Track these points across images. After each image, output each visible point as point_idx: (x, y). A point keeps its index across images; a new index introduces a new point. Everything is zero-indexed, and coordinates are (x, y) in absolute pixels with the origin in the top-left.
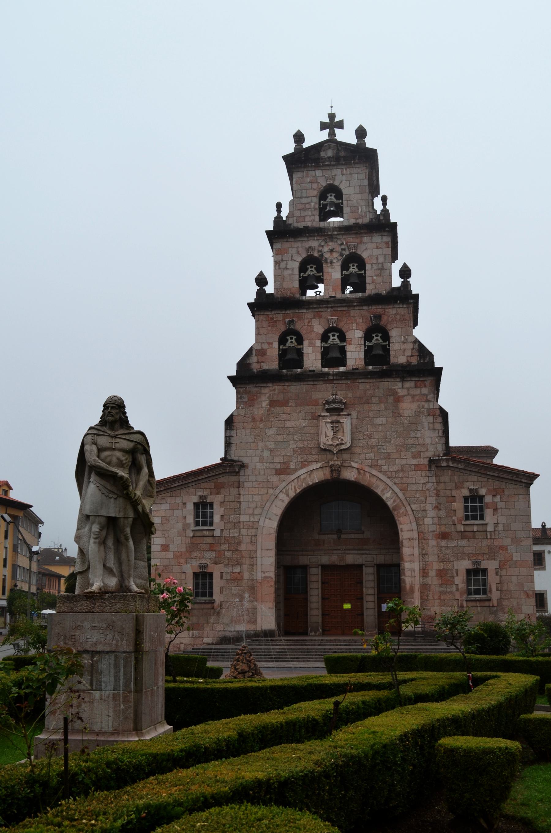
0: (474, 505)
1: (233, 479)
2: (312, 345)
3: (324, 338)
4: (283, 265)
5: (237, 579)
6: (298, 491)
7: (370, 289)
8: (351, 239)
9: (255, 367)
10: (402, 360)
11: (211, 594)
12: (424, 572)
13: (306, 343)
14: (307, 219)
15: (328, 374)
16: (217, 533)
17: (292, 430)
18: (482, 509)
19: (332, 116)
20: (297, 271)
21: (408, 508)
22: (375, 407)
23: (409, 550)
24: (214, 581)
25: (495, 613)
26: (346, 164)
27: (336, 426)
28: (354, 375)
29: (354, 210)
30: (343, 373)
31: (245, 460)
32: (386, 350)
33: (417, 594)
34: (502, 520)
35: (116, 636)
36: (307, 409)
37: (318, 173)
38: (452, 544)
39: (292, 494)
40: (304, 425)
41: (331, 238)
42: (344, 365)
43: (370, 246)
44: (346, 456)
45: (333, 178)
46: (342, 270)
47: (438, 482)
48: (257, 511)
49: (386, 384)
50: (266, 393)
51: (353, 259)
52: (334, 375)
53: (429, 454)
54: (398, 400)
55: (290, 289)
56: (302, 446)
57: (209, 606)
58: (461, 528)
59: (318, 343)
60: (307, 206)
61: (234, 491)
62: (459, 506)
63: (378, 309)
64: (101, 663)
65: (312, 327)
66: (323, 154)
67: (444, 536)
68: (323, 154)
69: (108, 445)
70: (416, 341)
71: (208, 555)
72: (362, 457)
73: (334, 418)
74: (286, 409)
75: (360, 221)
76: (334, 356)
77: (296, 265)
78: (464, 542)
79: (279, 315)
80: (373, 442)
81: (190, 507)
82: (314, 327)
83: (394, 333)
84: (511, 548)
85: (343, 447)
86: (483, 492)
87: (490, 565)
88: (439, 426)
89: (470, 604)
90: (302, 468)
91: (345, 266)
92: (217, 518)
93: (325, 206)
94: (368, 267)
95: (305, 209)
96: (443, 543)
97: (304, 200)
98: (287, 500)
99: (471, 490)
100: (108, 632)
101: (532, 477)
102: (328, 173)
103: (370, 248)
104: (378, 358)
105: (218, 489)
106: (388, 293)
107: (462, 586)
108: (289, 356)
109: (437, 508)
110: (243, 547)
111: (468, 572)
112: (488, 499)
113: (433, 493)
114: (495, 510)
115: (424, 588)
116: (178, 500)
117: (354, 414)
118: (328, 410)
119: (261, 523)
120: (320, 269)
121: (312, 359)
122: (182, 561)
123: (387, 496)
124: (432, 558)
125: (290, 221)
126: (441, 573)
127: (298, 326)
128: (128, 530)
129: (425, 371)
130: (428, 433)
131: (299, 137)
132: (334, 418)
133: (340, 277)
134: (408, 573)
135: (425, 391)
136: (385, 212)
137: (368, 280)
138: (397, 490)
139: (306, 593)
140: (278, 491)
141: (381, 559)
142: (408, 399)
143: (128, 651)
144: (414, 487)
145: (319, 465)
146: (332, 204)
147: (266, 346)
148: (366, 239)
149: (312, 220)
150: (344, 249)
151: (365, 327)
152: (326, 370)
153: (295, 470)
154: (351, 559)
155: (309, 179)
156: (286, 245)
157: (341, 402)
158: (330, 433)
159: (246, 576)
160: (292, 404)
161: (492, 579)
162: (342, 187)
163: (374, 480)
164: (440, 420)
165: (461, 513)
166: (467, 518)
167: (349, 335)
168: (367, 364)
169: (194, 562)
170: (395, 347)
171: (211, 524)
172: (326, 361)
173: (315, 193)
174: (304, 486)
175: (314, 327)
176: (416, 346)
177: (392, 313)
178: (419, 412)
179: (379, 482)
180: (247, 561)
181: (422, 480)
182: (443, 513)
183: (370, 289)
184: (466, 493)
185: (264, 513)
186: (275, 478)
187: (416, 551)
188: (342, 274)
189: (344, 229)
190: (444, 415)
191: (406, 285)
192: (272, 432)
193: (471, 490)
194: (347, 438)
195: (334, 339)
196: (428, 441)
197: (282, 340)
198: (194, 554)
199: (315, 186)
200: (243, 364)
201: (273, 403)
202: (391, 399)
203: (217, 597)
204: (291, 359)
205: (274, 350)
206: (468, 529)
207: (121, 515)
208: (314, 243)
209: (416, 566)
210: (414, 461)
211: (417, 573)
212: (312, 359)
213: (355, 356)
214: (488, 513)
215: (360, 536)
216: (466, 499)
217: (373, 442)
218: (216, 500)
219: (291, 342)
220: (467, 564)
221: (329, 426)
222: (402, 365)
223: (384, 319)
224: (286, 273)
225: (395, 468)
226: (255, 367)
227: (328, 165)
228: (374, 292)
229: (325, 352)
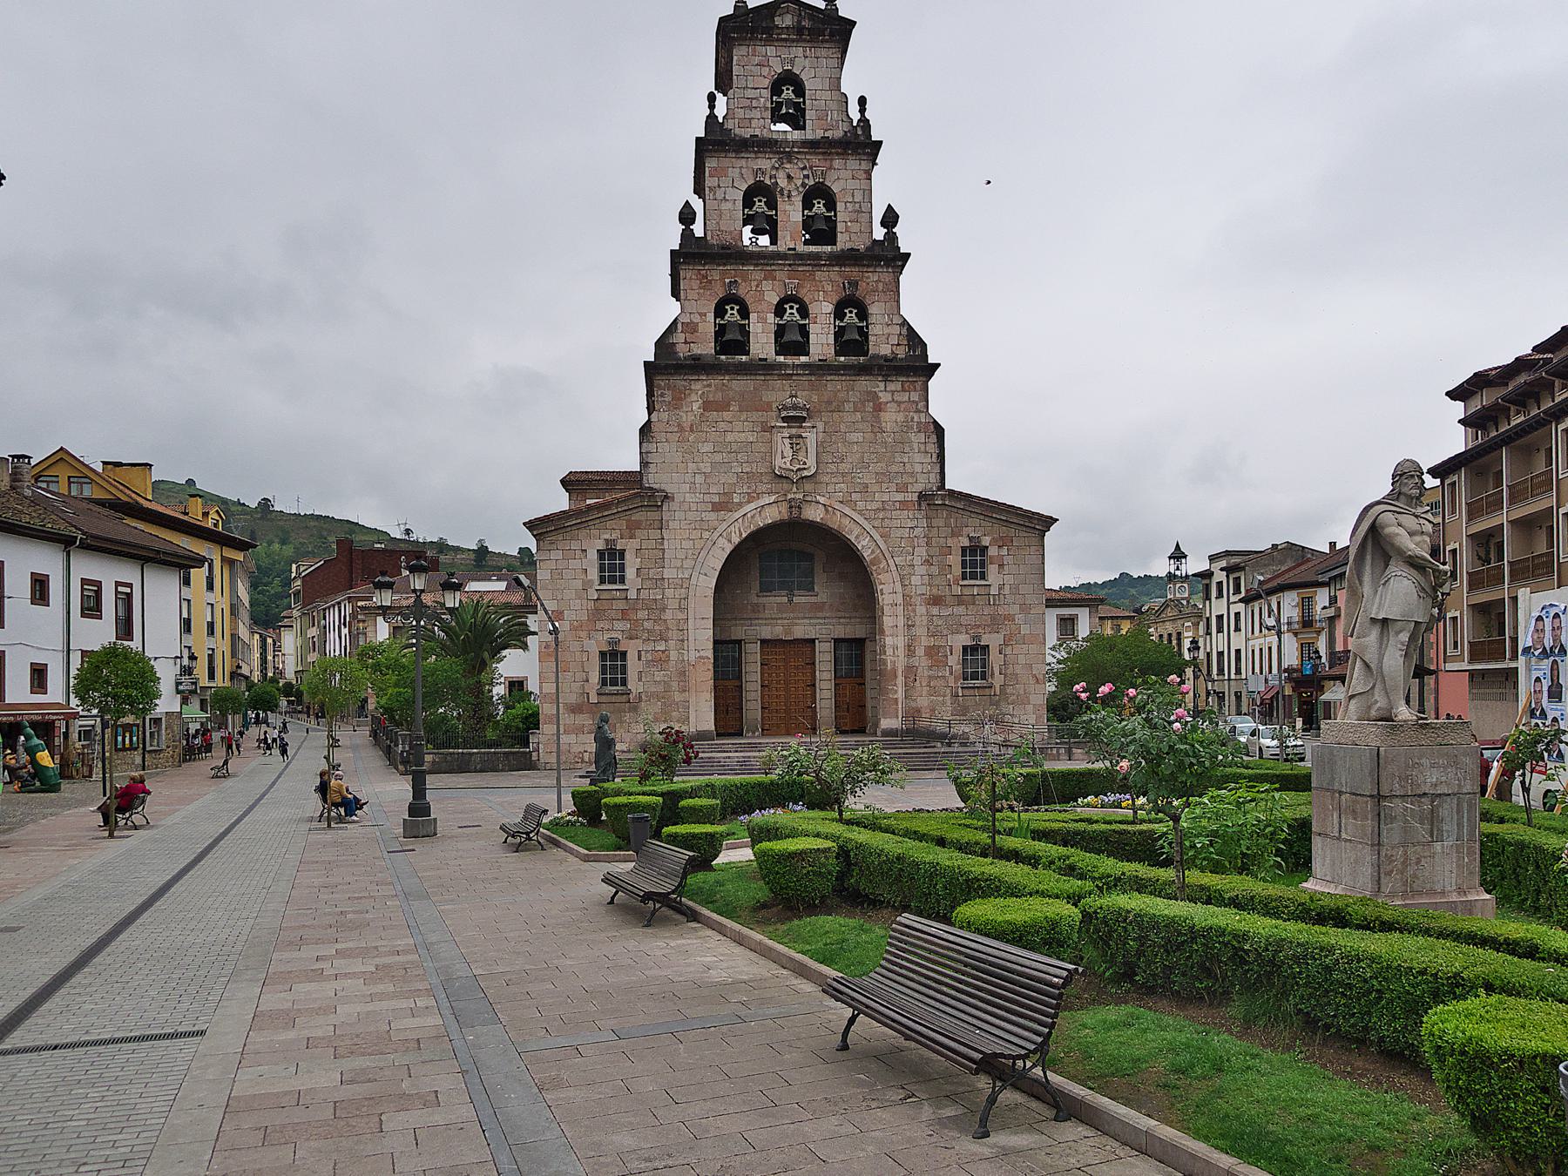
0: (975, 560)
1: (654, 515)
5: (661, 660)
7: (843, 242)
8: (815, 160)
9: (682, 351)
10: (885, 350)
11: (624, 683)
12: (910, 650)
13: (753, 316)
15: (786, 366)
16: (632, 595)
17: (734, 447)
18: (983, 565)
20: (740, 204)
21: (891, 562)
22: (848, 417)
23: (891, 618)
24: (629, 663)
25: (997, 704)
27: (796, 441)
28: (821, 369)
30: (804, 366)
31: (669, 489)
32: (864, 334)
33: (900, 680)
34: (1009, 579)
36: (755, 416)
37: (771, 51)
38: (945, 612)
39: (736, 540)
41: (789, 156)
42: (807, 354)
43: (843, 174)
44: (808, 487)
45: (792, 62)
47: (930, 527)
48: (688, 563)
49: (864, 384)
50: (699, 389)
51: (818, 193)
52: (794, 366)
53: (919, 487)
54: (879, 408)
57: (620, 699)
58: (957, 590)
59: (771, 317)
60: (755, 103)
61: (655, 534)
62: (955, 559)
63: (853, 272)
66: (778, 21)
67: (936, 601)
70: (905, 323)
71: (619, 625)
72: (831, 488)
73: (794, 431)
74: (726, 415)
76: (792, 341)
78: (961, 610)
79: (715, 273)
80: (844, 467)
81: (593, 555)
82: (764, 293)
83: (875, 310)
84: (1019, 618)
85: (806, 473)
86: (986, 541)
87: (992, 640)
88: (932, 448)
89: (967, 692)
92: (630, 573)
93: (780, 105)
94: (840, 207)
95: (751, 108)
96: (935, 610)
97: (750, 93)
98: (729, 548)
99: (971, 539)
101: (1049, 521)
102: (785, 53)
103: (840, 177)
104: (851, 343)
105: (632, 529)
106: (867, 249)
107: (958, 668)
108: (728, 337)
109: (928, 562)
110: (668, 615)
111: (965, 648)
112: (993, 551)
113: (923, 542)
114: (1001, 566)
115: (910, 671)
116: (575, 545)
117: (821, 426)
118: (784, 419)
119: (693, 581)
121: (762, 344)
122: (583, 634)
123: (864, 546)
124: (920, 631)
125: (729, 125)
126: (931, 651)
127: (742, 291)
129: (915, 365)
130: (918, 458)
132: (794, 431)
134: (889, 651)
135: (915, 396)
136: (865, 123)
137: (840, 227)
138: (877, 537)
139: (740, 677)
140: (716, 534)
141: (840, 632)
142: (892, 407)
144: (899, 533)
145: (773, 498)
146: (789, 101)
147: (696, 318)
148: (837, 163)
150: (807, 177)
151: (835, 299)
152: (781, 359)
153: (740, 505)
154: (800, 631)
155: (757, 60)
156: (725, 162)
157: (803, 408)
158: (789, 453)
159: (673, 655)
160: (734, 407)
161: (995, 659)
162: (803, 76)
163: (846, 521)
164: (934, 438)
165: (957, 570)
166: (964, 578)
167: (813, 309)
168: (838, 354)
169: (599, 636)
170: (876, 330)
171: (622, 581)
172: (783, 348)
173: (767, 83)
175: (764, 293)
176: (904, 331)
177: (873, 278)
178: (906, 426)
179: (853, 525)
180: (673, 634)
181: (910, 523)
182: (935, 570)
183: (843, 242)
184: (966, 543)
185: (697, 568)
186: (713, 516)
187: (901, 622)
189: (812, 145)
190: (939, 431)
191: (891, 238)
192: (707, 447)
193: (971, 539)
194: (811, 462)
195: (792, 313)
196: (918, 468)
197: (720, 312)
198: (599, 625)
199: (765, 71)
200: (663, 344)
201: (707, 406)
202: (869, 407)
203: (633, 685)
204: (732, 341)
205: (708, 326)
206: (967, 591)
208: (765, 163)
209: (901, 642)
210: (900, 497)
211: (901, 652)
212: (762, 344)
213: (821, 342)
214: (992, 570)
215: (813, 599)
216: (964, 549)
217: (844, 467)
218: (629, 546)
219: (732, 314)
220: (964, 639)
221: (787, 441)
222: (886, 359)
223: (862, 285)
224: (726, 206)
225: (875, 506)
226: (682, 351)
228: (848, 246)
229: (780, 332)
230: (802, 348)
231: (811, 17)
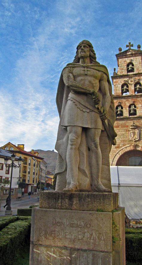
2: (126, 109)
3: (130, 107)
4: (116, 86)
6: (122, 153)
14: (123, 72)
15: (131, 118)
17: (120, 135)
19: (130, 43)
26: (135, 56)
29: (138, 69)
35: (94, 234)
37: (126, 59)
40: (124, 133)
41: (131, 77)
46: (134, 87)
52: (133, 118)
55: (119, 93)
56: (123, 139)
59: (128, 108)
60: (123, 69)
64: (80, 260)
65: (126, 104)
68: (128, 54)
69: (82, 72)
73: (133, 131)
75: (140, 72)
77: (121, 86)
85: (136, 140)
90: (123, 146)
91: (135, 85)
95: (123, 70)
100: (86, 230)
120: (128, 87)
128: (98, 140)
131: (120, 50)
132: (133, 131)
133: (134, 89)
143: (106, 250)
145: (129, 145)
149: (125, 73)
152: (131, 116)
153: (121, 147)
155: (123, 61)
158: (132, 136)
160: (120, 127)
167: (137, 106)
172: (130, 114)
173: (126, 65)
174: (124, 152)
186: (116, 149)
188: (134, 88)
199: (125, 63)
207: (93, 126)
208: (126, 79)
224: (117, 88)
227: (129, 57)
230: (135, 114)
231: (134, 52)
